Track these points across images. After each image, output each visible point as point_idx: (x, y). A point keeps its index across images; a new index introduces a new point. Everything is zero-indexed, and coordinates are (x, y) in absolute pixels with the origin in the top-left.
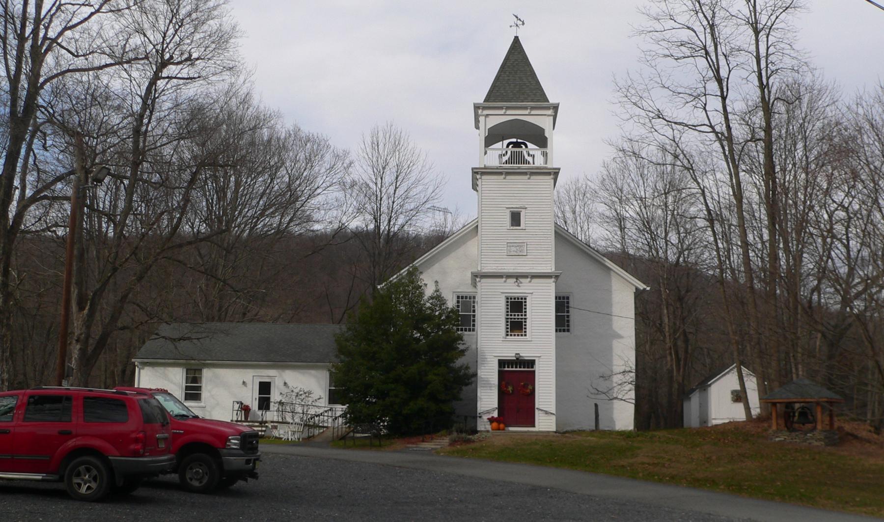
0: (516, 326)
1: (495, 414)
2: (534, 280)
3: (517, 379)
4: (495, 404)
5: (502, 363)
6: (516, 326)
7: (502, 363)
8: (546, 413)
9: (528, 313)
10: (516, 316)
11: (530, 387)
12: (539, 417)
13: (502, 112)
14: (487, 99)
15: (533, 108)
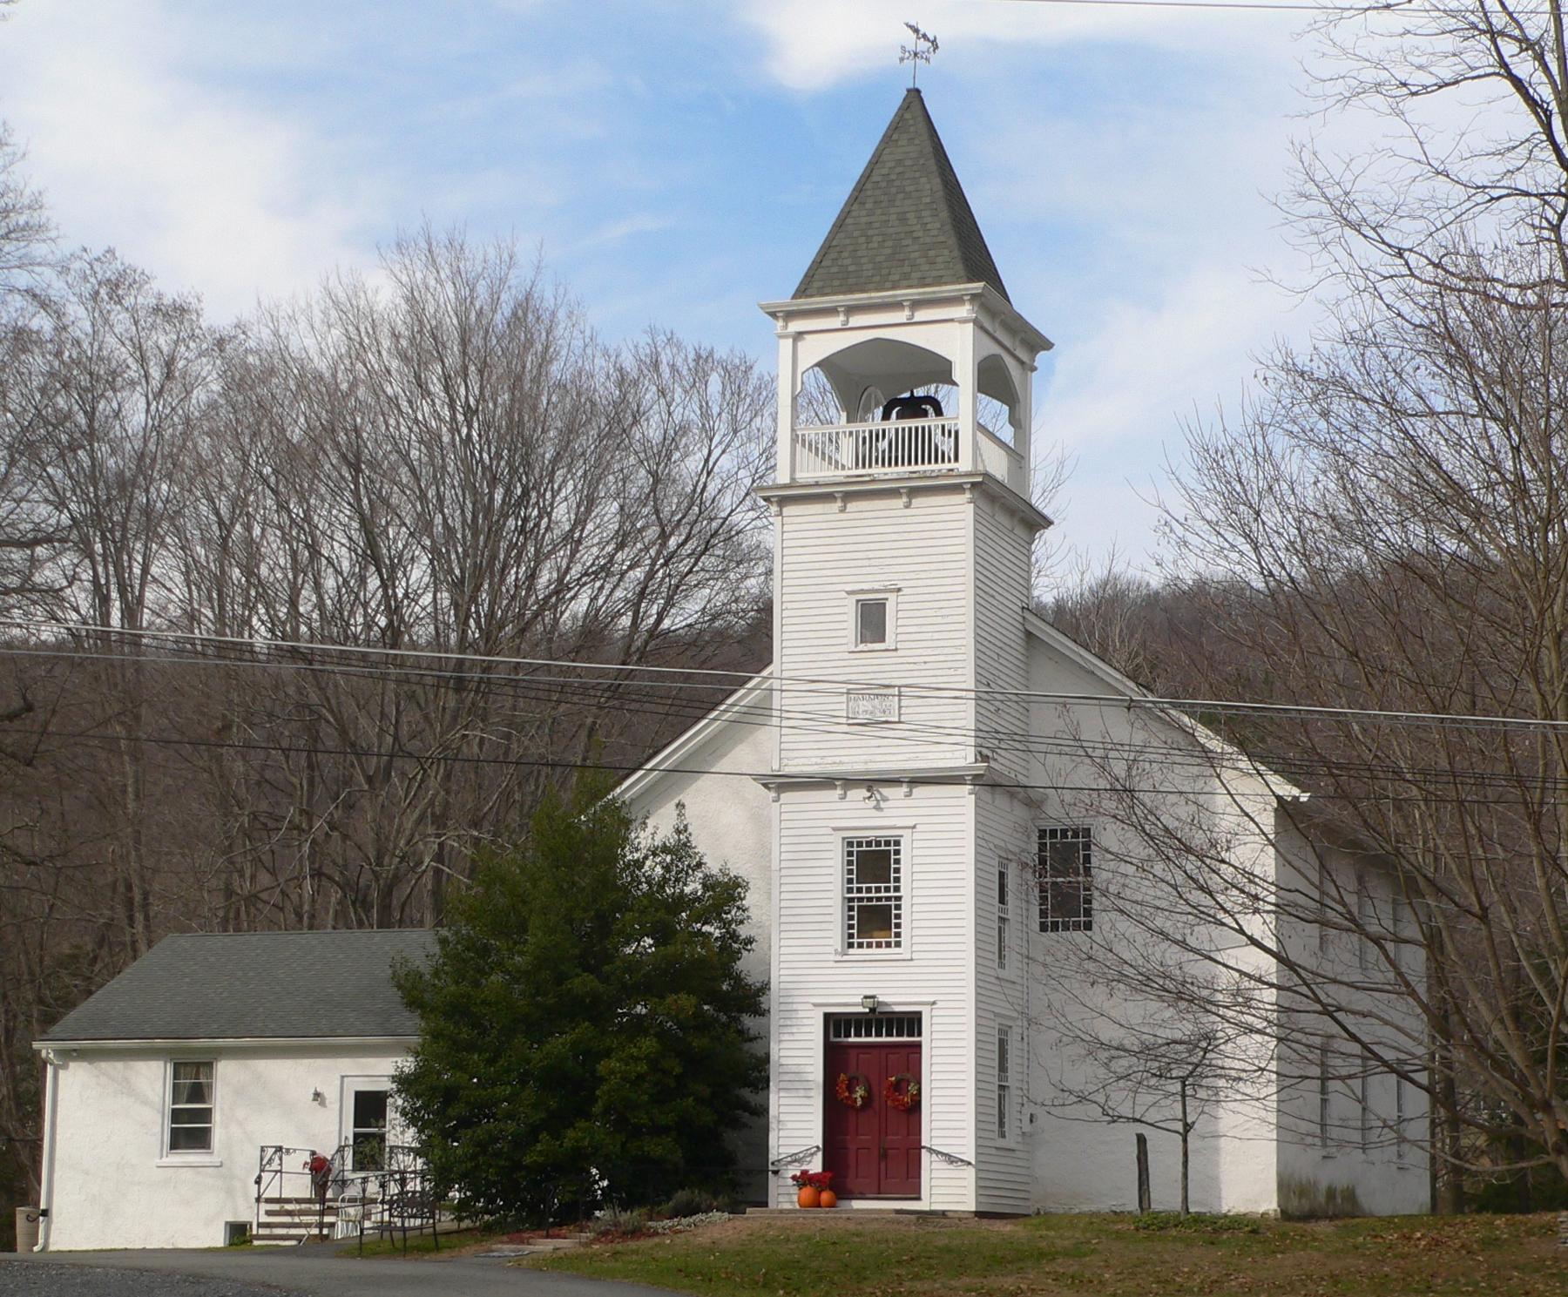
0: (873, 920)
1: (816, 1166)
2: (920, 791)
3: (873, 1065)
4: (817, 1139)
5: (836, 1024)
6: (873, 920)
7: (836, 1024)
8: (951, 1159)
9: (902, 884)
10: (873, 893)
11: (912, 1089)
12: (932, 1171)
13: (836, 322)
14: (801, 292)
15: (917, 304)
